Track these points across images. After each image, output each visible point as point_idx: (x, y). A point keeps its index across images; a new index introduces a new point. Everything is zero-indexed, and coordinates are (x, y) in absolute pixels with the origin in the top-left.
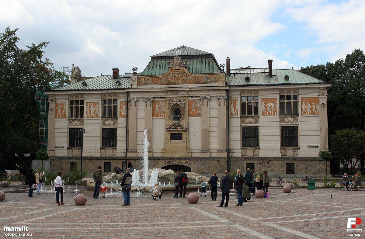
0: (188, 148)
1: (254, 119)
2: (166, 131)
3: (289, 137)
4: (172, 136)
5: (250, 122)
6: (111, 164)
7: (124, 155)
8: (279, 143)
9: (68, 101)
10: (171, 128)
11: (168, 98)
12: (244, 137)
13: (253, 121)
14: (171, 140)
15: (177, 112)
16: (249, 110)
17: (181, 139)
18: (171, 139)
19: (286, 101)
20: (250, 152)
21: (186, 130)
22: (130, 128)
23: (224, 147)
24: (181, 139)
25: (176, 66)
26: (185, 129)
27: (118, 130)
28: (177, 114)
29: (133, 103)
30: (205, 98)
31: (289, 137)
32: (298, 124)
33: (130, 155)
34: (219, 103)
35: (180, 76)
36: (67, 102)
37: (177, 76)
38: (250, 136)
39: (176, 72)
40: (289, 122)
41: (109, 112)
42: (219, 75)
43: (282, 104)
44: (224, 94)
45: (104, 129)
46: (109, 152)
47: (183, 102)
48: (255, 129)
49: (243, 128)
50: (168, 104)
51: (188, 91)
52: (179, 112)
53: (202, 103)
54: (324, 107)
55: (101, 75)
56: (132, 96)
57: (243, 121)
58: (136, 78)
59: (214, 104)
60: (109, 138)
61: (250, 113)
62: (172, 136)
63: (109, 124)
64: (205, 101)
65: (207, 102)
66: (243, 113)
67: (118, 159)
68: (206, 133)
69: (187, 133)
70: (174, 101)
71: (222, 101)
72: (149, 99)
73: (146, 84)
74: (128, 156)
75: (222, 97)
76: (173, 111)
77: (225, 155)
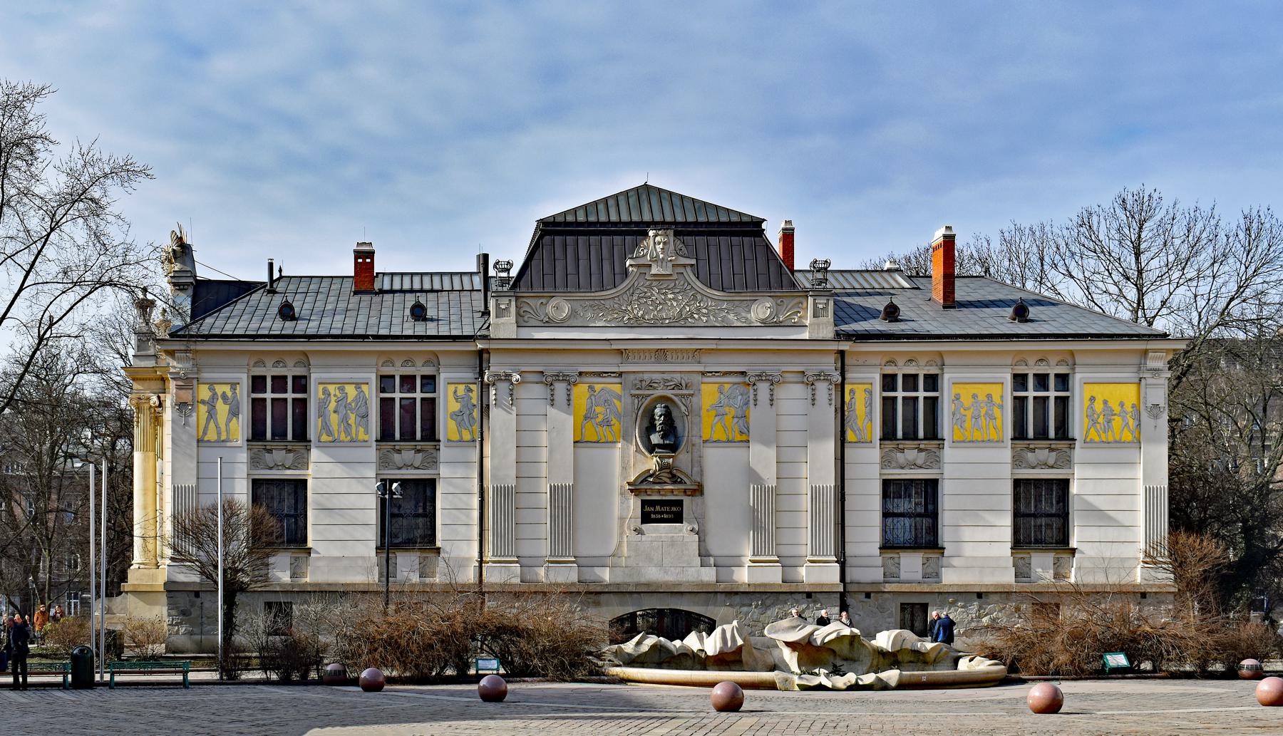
3: (1042, 515)
4: (647, 509)
10: (645, 480)
11: (632, 377)
14: (643, 522)
16: (914, 419)
18: (643, 522)
19: (1031, 393)
21: (698, 490)
24: (678, 518)
31: (1042, 515)
35: (670, 296)
38: (915, 514)
39: (655, 283)
41: (408, 423)
44: (829, 365)
47: (685, 392)
48: (930, 488)
50: (633, 396)
53: (752, 397)
54: (1156, 417)
56: (496, 366)
57: (885, 462)
59: (792, 396)
62: (647, 509)
63: (408, 464)
64: (763, 388)
66: (888, 434)
69: (698, 499)
72: (558, 377)
74: (486, 578)
75: (819, 376)
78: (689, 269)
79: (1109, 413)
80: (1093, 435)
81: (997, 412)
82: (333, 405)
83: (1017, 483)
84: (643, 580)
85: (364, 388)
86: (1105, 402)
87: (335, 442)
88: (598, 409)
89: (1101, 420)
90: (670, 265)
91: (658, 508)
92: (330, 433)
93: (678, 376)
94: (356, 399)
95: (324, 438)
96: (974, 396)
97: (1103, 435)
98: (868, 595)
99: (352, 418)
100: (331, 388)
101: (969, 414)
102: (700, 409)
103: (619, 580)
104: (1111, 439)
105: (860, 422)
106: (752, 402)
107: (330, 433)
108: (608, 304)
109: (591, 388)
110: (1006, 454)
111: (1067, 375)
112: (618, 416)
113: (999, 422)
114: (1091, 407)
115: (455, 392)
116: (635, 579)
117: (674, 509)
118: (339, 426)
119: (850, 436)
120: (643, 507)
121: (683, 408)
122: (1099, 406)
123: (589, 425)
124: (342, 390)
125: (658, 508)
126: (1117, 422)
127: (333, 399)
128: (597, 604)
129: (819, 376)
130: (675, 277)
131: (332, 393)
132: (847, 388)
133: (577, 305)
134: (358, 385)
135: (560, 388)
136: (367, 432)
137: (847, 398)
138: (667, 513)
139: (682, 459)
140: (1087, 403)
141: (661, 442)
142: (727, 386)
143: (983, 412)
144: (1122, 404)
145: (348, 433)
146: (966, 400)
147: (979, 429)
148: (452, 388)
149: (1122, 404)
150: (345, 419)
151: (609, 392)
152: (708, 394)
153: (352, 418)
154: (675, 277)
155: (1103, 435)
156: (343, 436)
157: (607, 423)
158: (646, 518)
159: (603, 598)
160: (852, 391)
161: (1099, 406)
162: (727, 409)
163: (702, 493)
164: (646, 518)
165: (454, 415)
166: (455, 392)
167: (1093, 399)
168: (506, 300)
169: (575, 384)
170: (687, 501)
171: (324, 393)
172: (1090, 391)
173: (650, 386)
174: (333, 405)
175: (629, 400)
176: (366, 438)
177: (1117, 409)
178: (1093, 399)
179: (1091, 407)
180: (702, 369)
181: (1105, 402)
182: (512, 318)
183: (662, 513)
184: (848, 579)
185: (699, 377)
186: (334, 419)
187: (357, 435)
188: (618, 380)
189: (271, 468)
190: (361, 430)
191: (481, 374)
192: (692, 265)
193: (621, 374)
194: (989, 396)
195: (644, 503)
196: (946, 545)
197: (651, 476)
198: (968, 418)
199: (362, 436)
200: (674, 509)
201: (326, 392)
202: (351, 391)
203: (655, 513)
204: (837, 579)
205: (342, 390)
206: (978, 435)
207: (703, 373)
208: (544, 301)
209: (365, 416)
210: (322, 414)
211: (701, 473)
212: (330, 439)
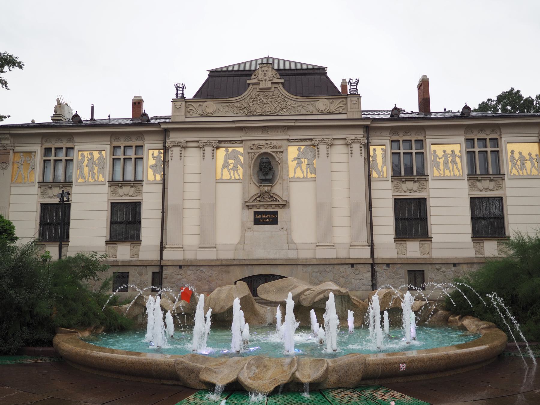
0: (290, 241)
1: (417, 184)
2: (246, 208)
4: (257, 216)
5: (410, 190)
6: (128, 276)
7: (156, 256)
8: (468, 229)
9: (39, 148)
10: (255, 199)
11: (249, 144)
12: (399, 220)
13: (415, 189)
15: (266, 169)
17: (275, 221)
20: (413, 250)
21: (285, 205)
22: (171, 202)
23: (364, 239)
24: (275, 221)
25: (264, 82)
26: (284, 203)
27: (144, 206)
28: (266, 174)
29: (176, 151)
30: (322, 142)
32: (503, 192)
33: (168, 255)
34: (350, 152)
36: (39, 150)
37: (265, 101)
38: (412, 219)
39: (262, 93)
40: (486, 189)
42: (349, 99)
43: (471, 154)
45: (114, 205)
46: (123, 252)
49: (398, 202)
50: (249, 153)
51: (289, 128)
52: (271, 169)
53: (317, 153)
55: (109, 116)
58: (184, 103)
60: (125, 221)
61: (409, 171)
62: (257, 216)
64: (323, 148)
65: (326, 150)
66: (396, 174)
67: (145, 265)
68: (324, 213)
70: (261, 148)
71: (356, 147)
73: (202, 116)
74: (165, 257)
75: (356, 141)
76: (257, 169)
77: (366, 253)
78: (281, 85)
79: (522, 158)
80: (514, 171)
81: (458, 160)
82: (86, 162)
83: (472, 200)
84: (255, 258)
85: (103, 153)
86: (520, 153)
87: (86, 184)
88: (231, 161)
89: (518, 163)
90: (270, 82)
91: (263, 216)
92: (83, 177)
93: (274, 143)
94: (98, 159)
95: (80, 180)
96: (444, 151)
97: (521, 172)
98: (388, 265)
99: (96, 169)
100: (86, 153)
101: (442, 161)
102: (287, 160)
103: (241, 258)
104: (525, 174)
105: (380, 167)
106: (317, 156)
107: (83, 177)
108: (237, 105)
109: (227, 151)
110: (465, 183)
111: (497, 139)
112: (242, 166)
113: (459, 166)
114: (512, 156)
115: (153, 154)
116: (250, 257)
117: (273, 216)
118: (89, 173)
119: (374, 175)
120: (255, 216)
121: (277, 159)
122: (517, 156)
123: (225, 170)
124: (91, 154)
125: (263, 216)
126: (528, 164)
127: (86, 159)
128: (228, 272)
129: (356, 141)
130: (273, 89)
131: (86, 156)
132: (371, 148)
133: (219, 106)
134: (100, 151)
135: (208, 150)
136: (103, 177)
137: (371, 153)
138: (269, 218)
139: (277, 190)
140: (509, 154)
141: (264, 178)
142: (303, 148)
143: (450, 159)
144: (530, 154)
145: (93, 177)
146: (440, 153)
147: (449, 169)
148: (151, 152)
149: (530, 154)
150: (91, 170)
151: (237, 151)
152: (293, 152)
153: (96, 169)
154: (273, 89)
155: (521, 172)
156: (90, 179)
157: (235, 169)
158: (257, 222)
159: (231, 268)
160: (374, 150)
161: (517, 156)
162: (303, 160)
163: (289, 207)
164: (257, 222)
165: (152, 167)
166: (153, 154)
167: (513, 152)
168: (179, 103)
169: (218, 148)
170: (281, 212)
171: (81, 156)
172: (510, 147)
173: (259, 148)
174: (86, 162)
175: (247, 156)
176: (103, 180)
177: (527, 157)
178: (513, 152)
179: (512, 156)
180: (288, 138)
181: (520, 153)
182: (183, 113)
183: (266, 219)
184: (376, 256)
185: (286, 142)
186: (86, 169)
187: (98, 178)
188: (241, 145)
189: (51, 197)
190: (101, 175)
191: (165, 143)
192: (282, 83)
193: (242, 141)
194: (453, 151)
195: (255, 213)
196: (433, 236)
197: (259, 197)
198: (441, 163)
199: (101, 179)
200: (273, 216)
201: (83, 156)
202: (96, 154)
203: (262, 218)
204: (368, 255)
205: (91, 154)
206: (447, 173)
207: (288, 140)
208: (201, 103)
209: (102, 168)
210: (80, 167)
211: (289, 196)
212: (84, 180)
